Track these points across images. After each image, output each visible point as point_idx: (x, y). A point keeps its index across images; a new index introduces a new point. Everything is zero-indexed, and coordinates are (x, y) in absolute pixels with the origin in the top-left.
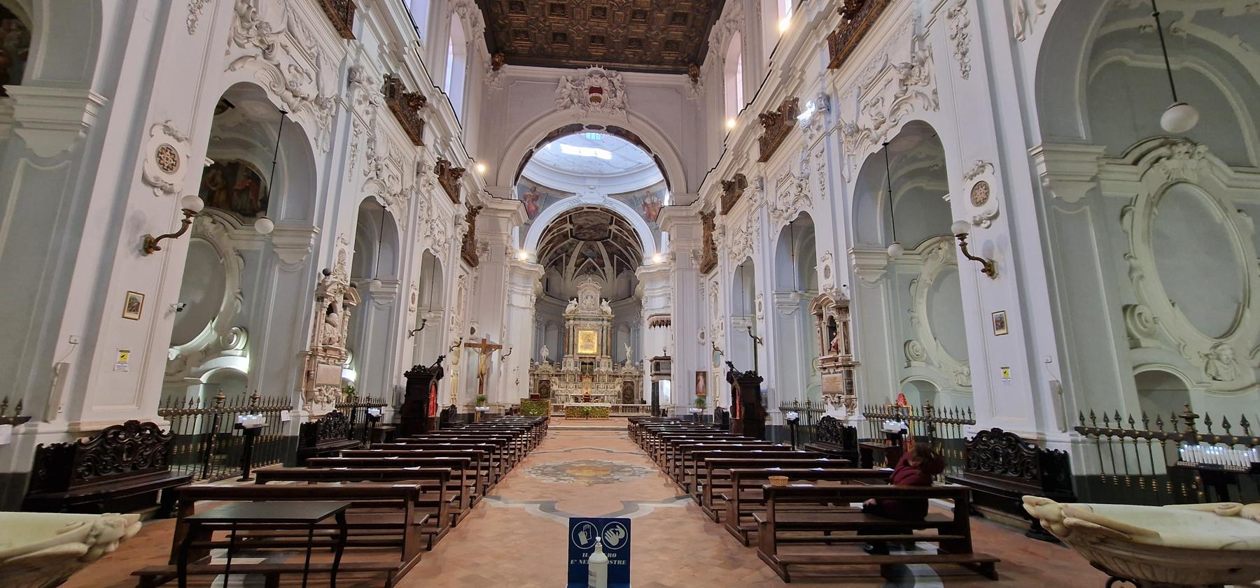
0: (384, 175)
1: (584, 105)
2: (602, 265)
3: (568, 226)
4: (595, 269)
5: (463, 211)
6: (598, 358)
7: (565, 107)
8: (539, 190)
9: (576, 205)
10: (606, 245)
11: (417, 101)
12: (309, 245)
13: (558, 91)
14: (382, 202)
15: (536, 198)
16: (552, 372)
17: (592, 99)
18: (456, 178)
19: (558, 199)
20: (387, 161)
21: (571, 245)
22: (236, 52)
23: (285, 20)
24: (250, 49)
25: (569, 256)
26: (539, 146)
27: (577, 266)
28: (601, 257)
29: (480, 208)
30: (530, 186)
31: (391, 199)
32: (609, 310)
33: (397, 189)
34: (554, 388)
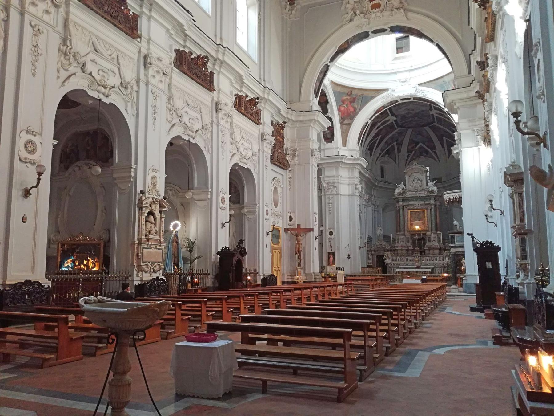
0: (185, 119)
1: (365, 14)
2: (433, 148)
3: (391, 119)
4: (427, 152)
5: (269, 130)
6: (429, 233)
7: (351, 21)
8: (354, 92)
9: (389, 100)
10: (434, 129)
11: (202, 60)
12: (130, 176)
13: (343, 8)
14: (187, 138)
15: (353, 100)
16: (388, 248)
17: (373, 7)
18: (255, 105)
19: (373, 97)
20: (186, 109)
21: (400, 133)
22: (64, 74)
23: (91, 44)
24: (72, 69)
25: (400, 144)
26: (333, 59)
27: (409, 151)
28: (430, 140)
29: (284, 123)
30: (346, 91)
31: (193, 134)
32: (435, 189)
33: (198, 126)
34: (388, 261)
